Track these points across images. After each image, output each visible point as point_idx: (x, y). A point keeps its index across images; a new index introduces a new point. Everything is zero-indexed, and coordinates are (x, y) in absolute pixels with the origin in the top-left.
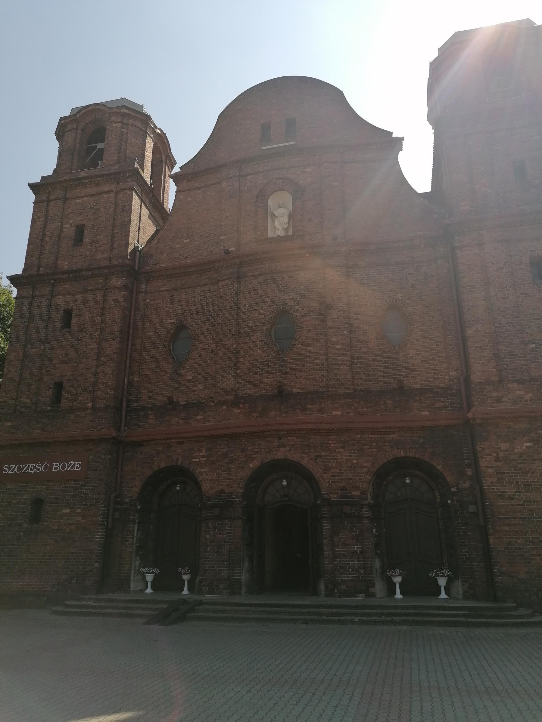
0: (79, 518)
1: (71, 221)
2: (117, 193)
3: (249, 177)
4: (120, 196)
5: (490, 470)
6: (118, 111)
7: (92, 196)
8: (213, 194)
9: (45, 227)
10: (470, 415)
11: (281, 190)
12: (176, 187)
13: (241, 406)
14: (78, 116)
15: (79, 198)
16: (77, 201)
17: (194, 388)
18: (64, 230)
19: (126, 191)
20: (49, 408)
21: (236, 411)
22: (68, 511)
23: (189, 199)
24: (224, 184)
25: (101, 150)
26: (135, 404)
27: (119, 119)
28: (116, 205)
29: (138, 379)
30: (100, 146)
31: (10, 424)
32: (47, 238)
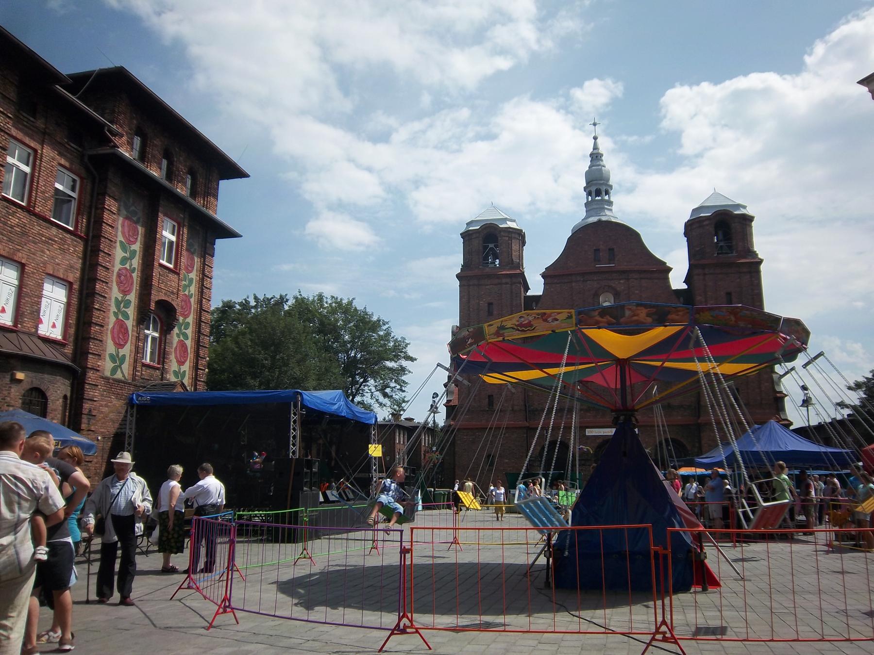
0: (514, 464)
1: (484, 300)
2: (511, 284)
3: (588, 282)
4: (514, 287)
5: (706, 445)
6: (506, 230)
7: (495, 285)
8: (567, 288)
9: (469, 302)
10: (699, 421)
11: (607, 292)
12: (543, 280)
13: (592, 412)
14: (480, 229)
15: (487, 285)
16: (487, 287)
17: (564, 401)
18: (480, 305)
19: (516, 284)
20: (487, 409)
21: (589, 414)
22: (507, 461)
23: (552, 289)
24: (574, 284)
25: (491, 248)
26: (532, 408)
27: (507, 235)
28: (512, 292)
29: (531, 394)
30: (491, 246)
31: (467, 416)
32: (471, 310)
